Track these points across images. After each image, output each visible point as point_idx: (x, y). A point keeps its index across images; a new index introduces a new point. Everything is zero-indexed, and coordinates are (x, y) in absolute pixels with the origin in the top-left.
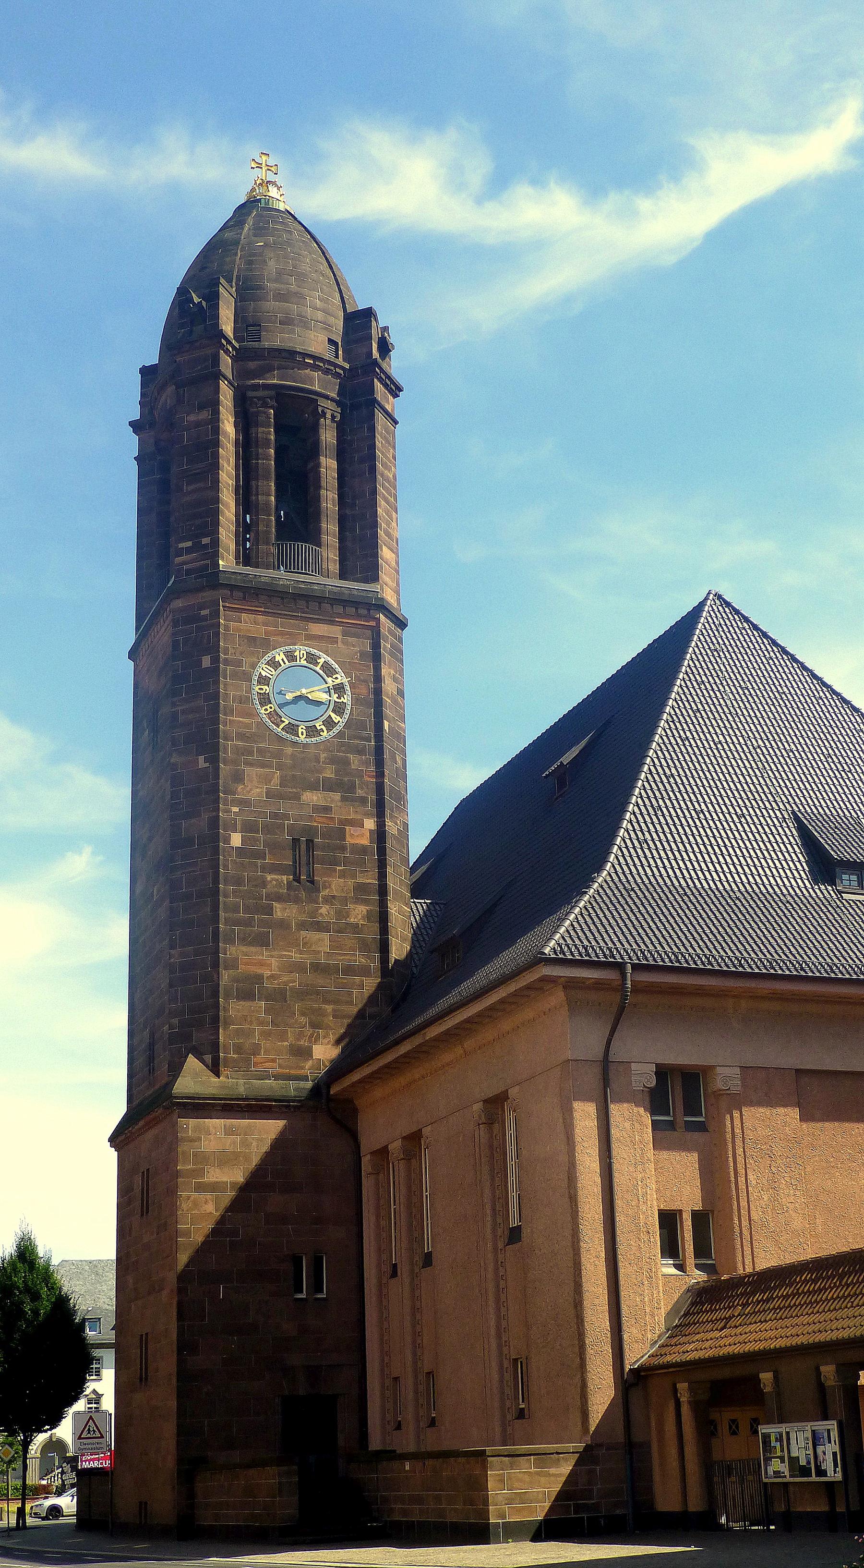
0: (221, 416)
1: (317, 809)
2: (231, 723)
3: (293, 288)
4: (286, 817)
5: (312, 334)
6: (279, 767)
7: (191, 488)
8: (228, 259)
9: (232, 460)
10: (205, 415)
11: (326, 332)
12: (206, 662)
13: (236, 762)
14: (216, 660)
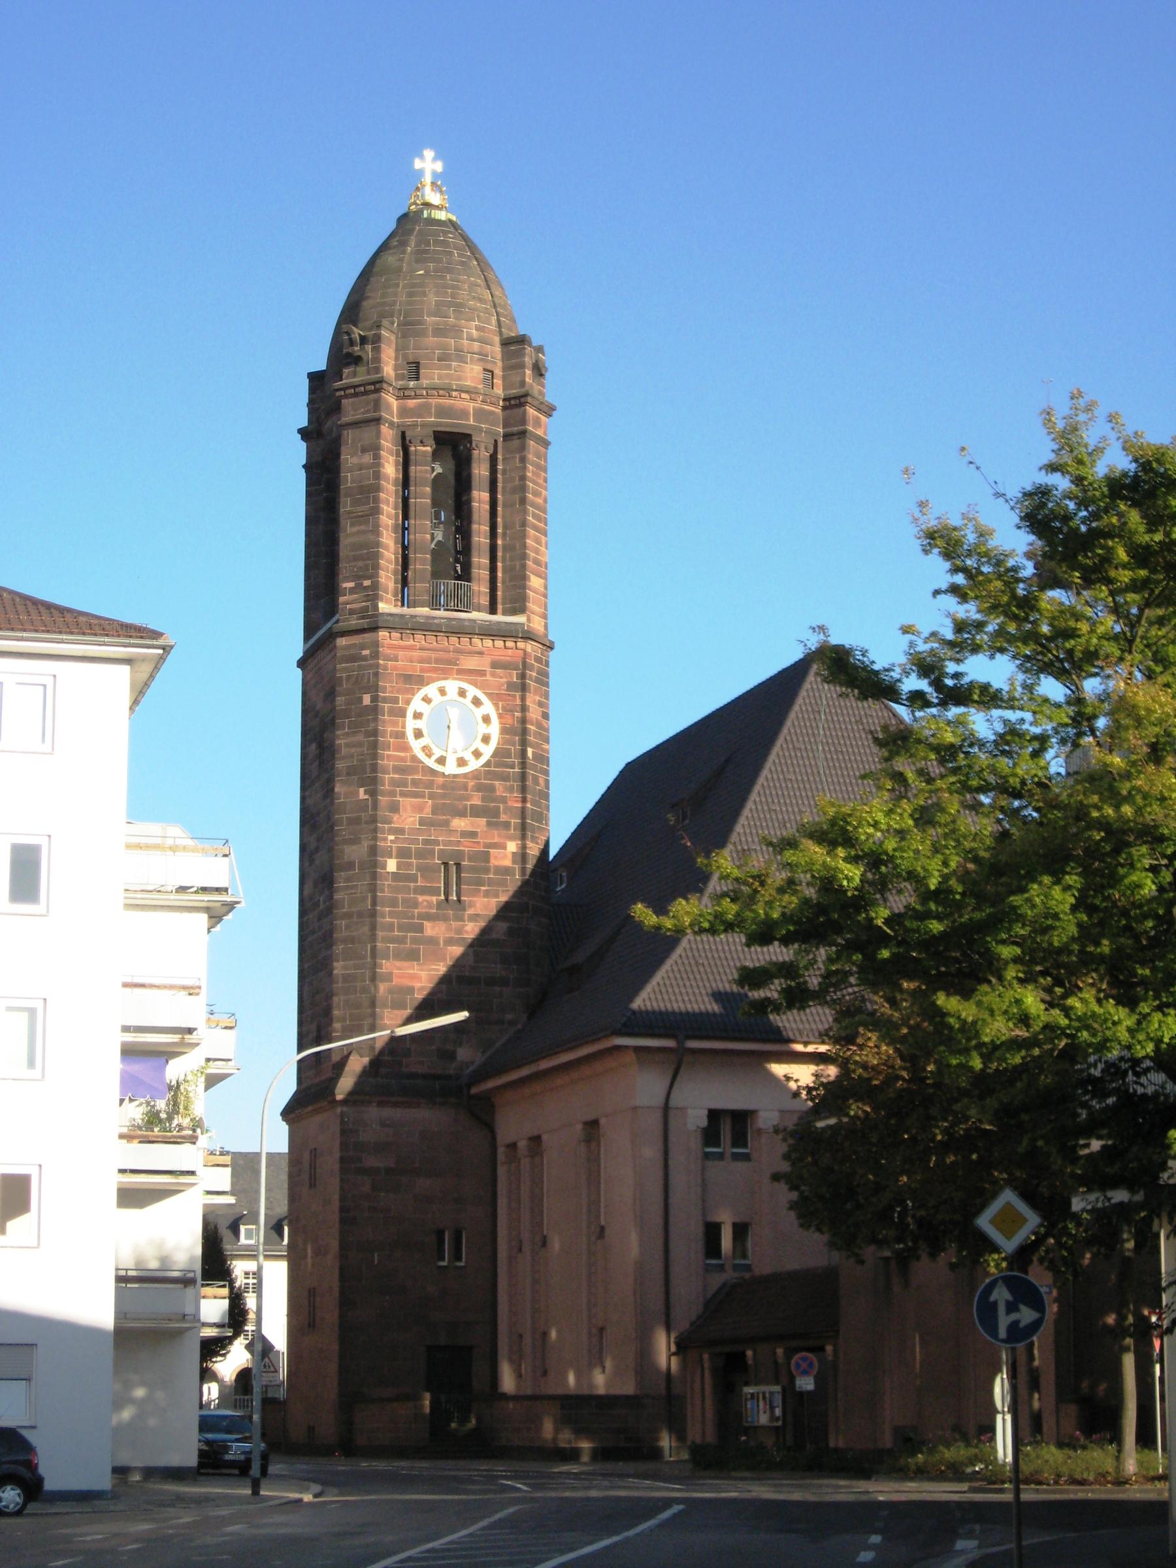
1: (465, 834)
2: (389, 757)
4: (437, 843)
6: (432, 796)
7: (355, 529)
9: (392, 500)
10: (367, 459)
12: (367, 700)
13: (392, 794)
14: (375, 699)
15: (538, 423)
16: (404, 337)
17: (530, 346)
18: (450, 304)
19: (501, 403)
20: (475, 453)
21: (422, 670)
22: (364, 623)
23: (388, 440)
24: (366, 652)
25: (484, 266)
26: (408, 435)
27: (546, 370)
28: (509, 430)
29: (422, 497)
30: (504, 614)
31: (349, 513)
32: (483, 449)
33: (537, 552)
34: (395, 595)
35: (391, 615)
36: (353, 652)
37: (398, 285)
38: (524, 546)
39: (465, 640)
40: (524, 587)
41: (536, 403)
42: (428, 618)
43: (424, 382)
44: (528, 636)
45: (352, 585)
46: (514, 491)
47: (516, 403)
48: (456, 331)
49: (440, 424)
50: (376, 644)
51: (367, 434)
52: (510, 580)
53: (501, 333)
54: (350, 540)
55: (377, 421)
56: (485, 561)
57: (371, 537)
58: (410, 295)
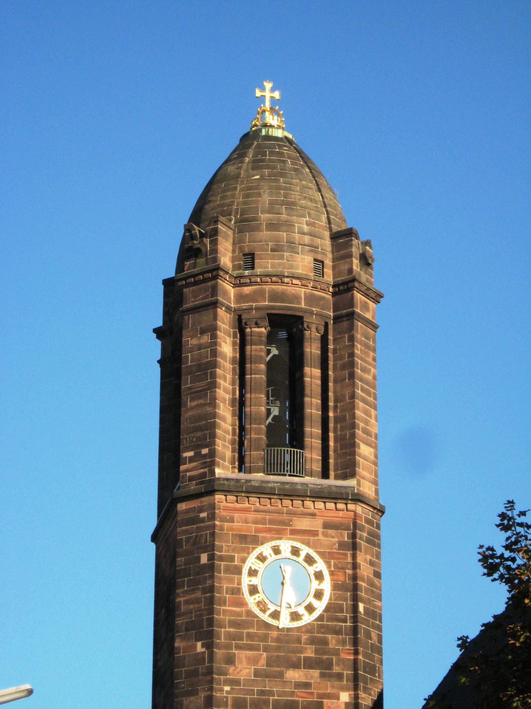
0: (218, 340)
1: (299, 685)
2: (225, 612)
3: (284, 217)
4: (271, 693)
5: (299, 257)
6: (266, 649)
7: (194, 403)
8: (229, 193)
9: (229, 376)
10: (206, 339)
11: (312, 254)
12: (204, 558)
13: (228, 647)
14: (211, 558)
15: (366, 307)
16: (241, 231)
17: (357, 238)
18: (283, 203)
19: (331, 289)
20: (307, 333)
21: (257, 530)
22: (202, 488)
23: (224, 321)
24: (204, 515)
25: (315, 173)
26: (244, 316)
27: (373, 260)
28: (339, 313)
29: (258, 374)
30: (337, 478)
31: (189, 388)
32: (314, 329)
33: (367, 423)
34: (233, 463)
35: (228, 480)
36: (192, 515)
37: (235, 188)
38: (353, 416)
39: (298, 503)
40: (353, 454)
41: (363, 288)
42: (263, 482)
43: (258, 270)
44: (358, 499)
45: (191, 454)
46: (343, 367)
47: (344, 288)
48: (289, 226)
49: (273, 308)
50: (212, 507)
51: (205, 317)
52: (341, 449)
53: (330, 229)
54: (190, 413)
55: (215, 304)
56: (317, 431)
57: (209, 409)
58: (247, 196)
